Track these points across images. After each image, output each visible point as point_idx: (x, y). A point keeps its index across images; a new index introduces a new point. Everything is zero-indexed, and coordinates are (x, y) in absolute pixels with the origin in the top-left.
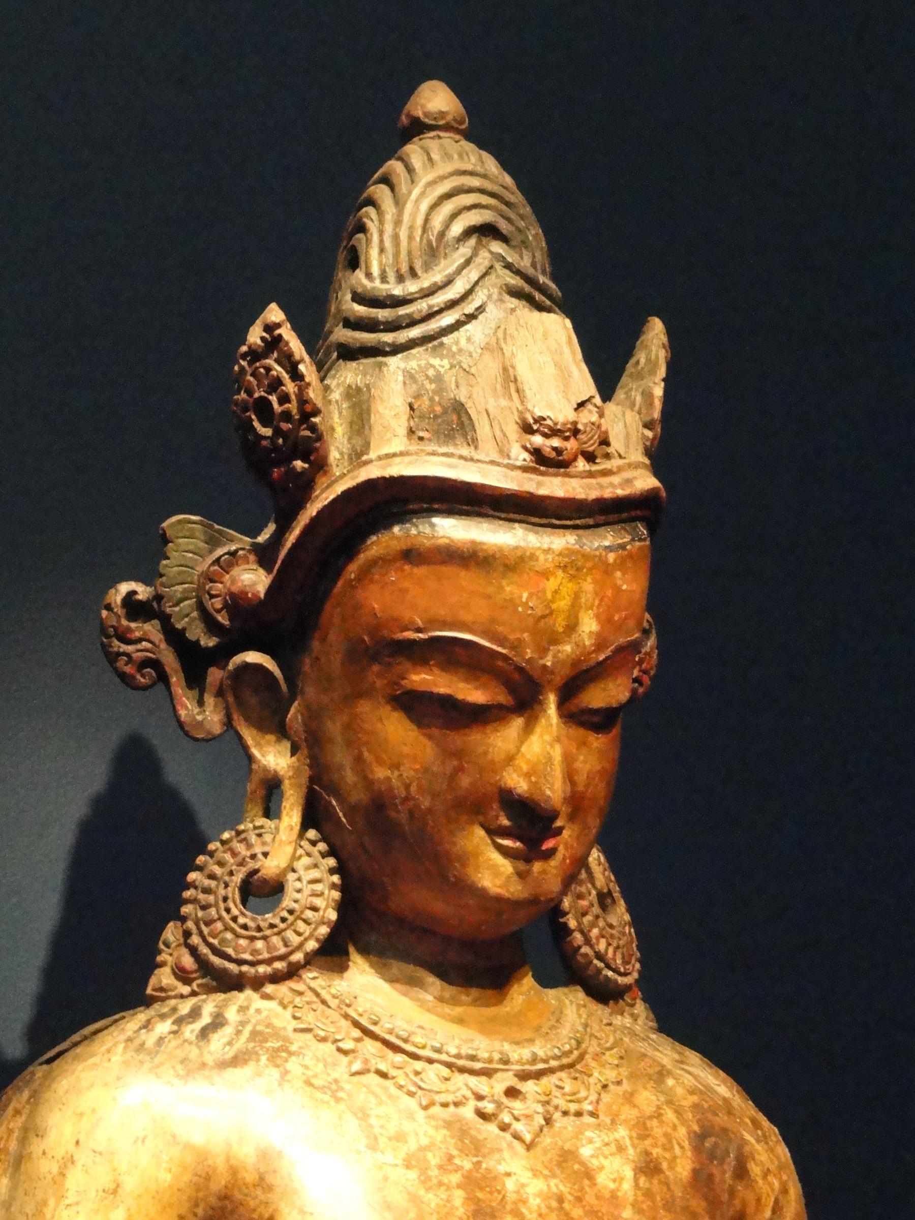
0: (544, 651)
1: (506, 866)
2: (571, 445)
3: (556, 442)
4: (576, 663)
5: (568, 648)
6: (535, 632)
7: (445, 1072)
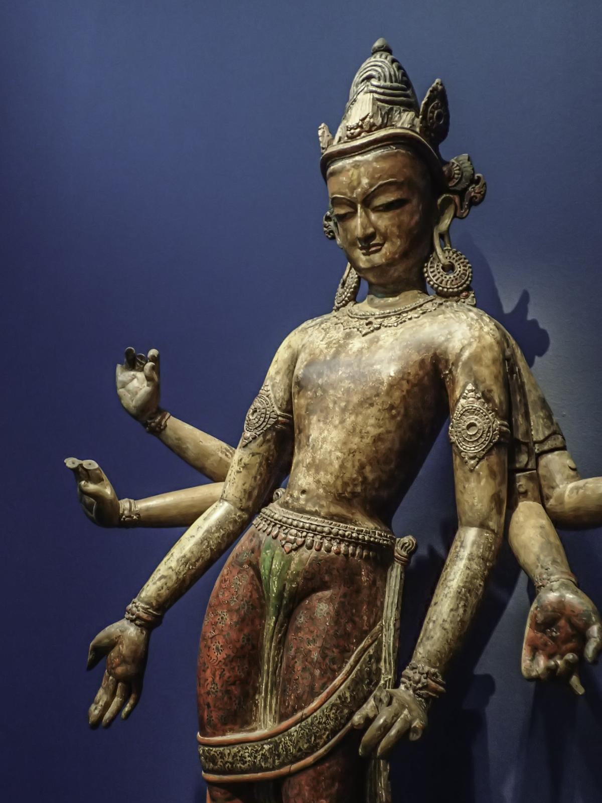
0: (352, 193)
1: (363, 258)
2: (358, 130)
3: (352, 131)
4: (364, 193)
5: (359, 190)
6: (348, 188)
7: (356, 319)
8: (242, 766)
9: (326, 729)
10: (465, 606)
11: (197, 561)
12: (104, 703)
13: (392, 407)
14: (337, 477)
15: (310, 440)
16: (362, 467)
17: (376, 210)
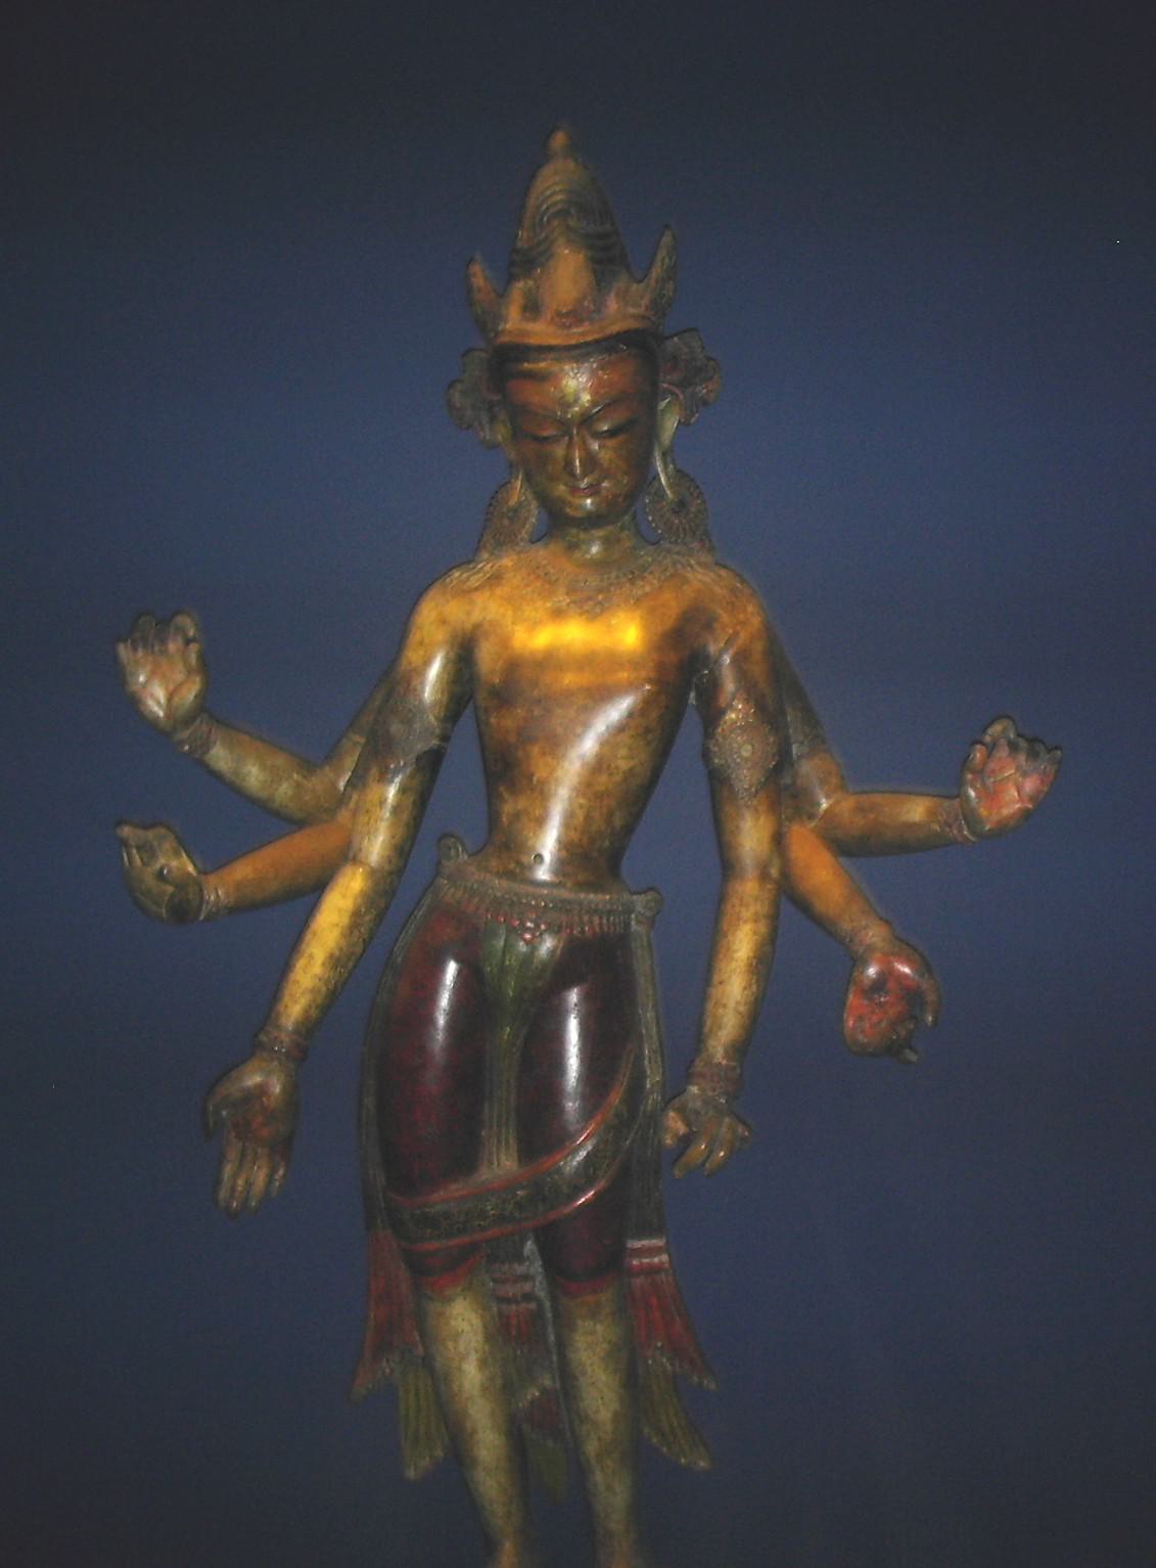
0: (566, 412)
4: (582, 415)
5: (577, 409)
8: (482, 1223)
9: (605, 1157)
10: (757, 981)
11: (349, 959)
12: (249, 1177)
13: (647, 730)
14: (583, 833)
15: (535, 782)
16: (611, 814)
17: (598, 435)
